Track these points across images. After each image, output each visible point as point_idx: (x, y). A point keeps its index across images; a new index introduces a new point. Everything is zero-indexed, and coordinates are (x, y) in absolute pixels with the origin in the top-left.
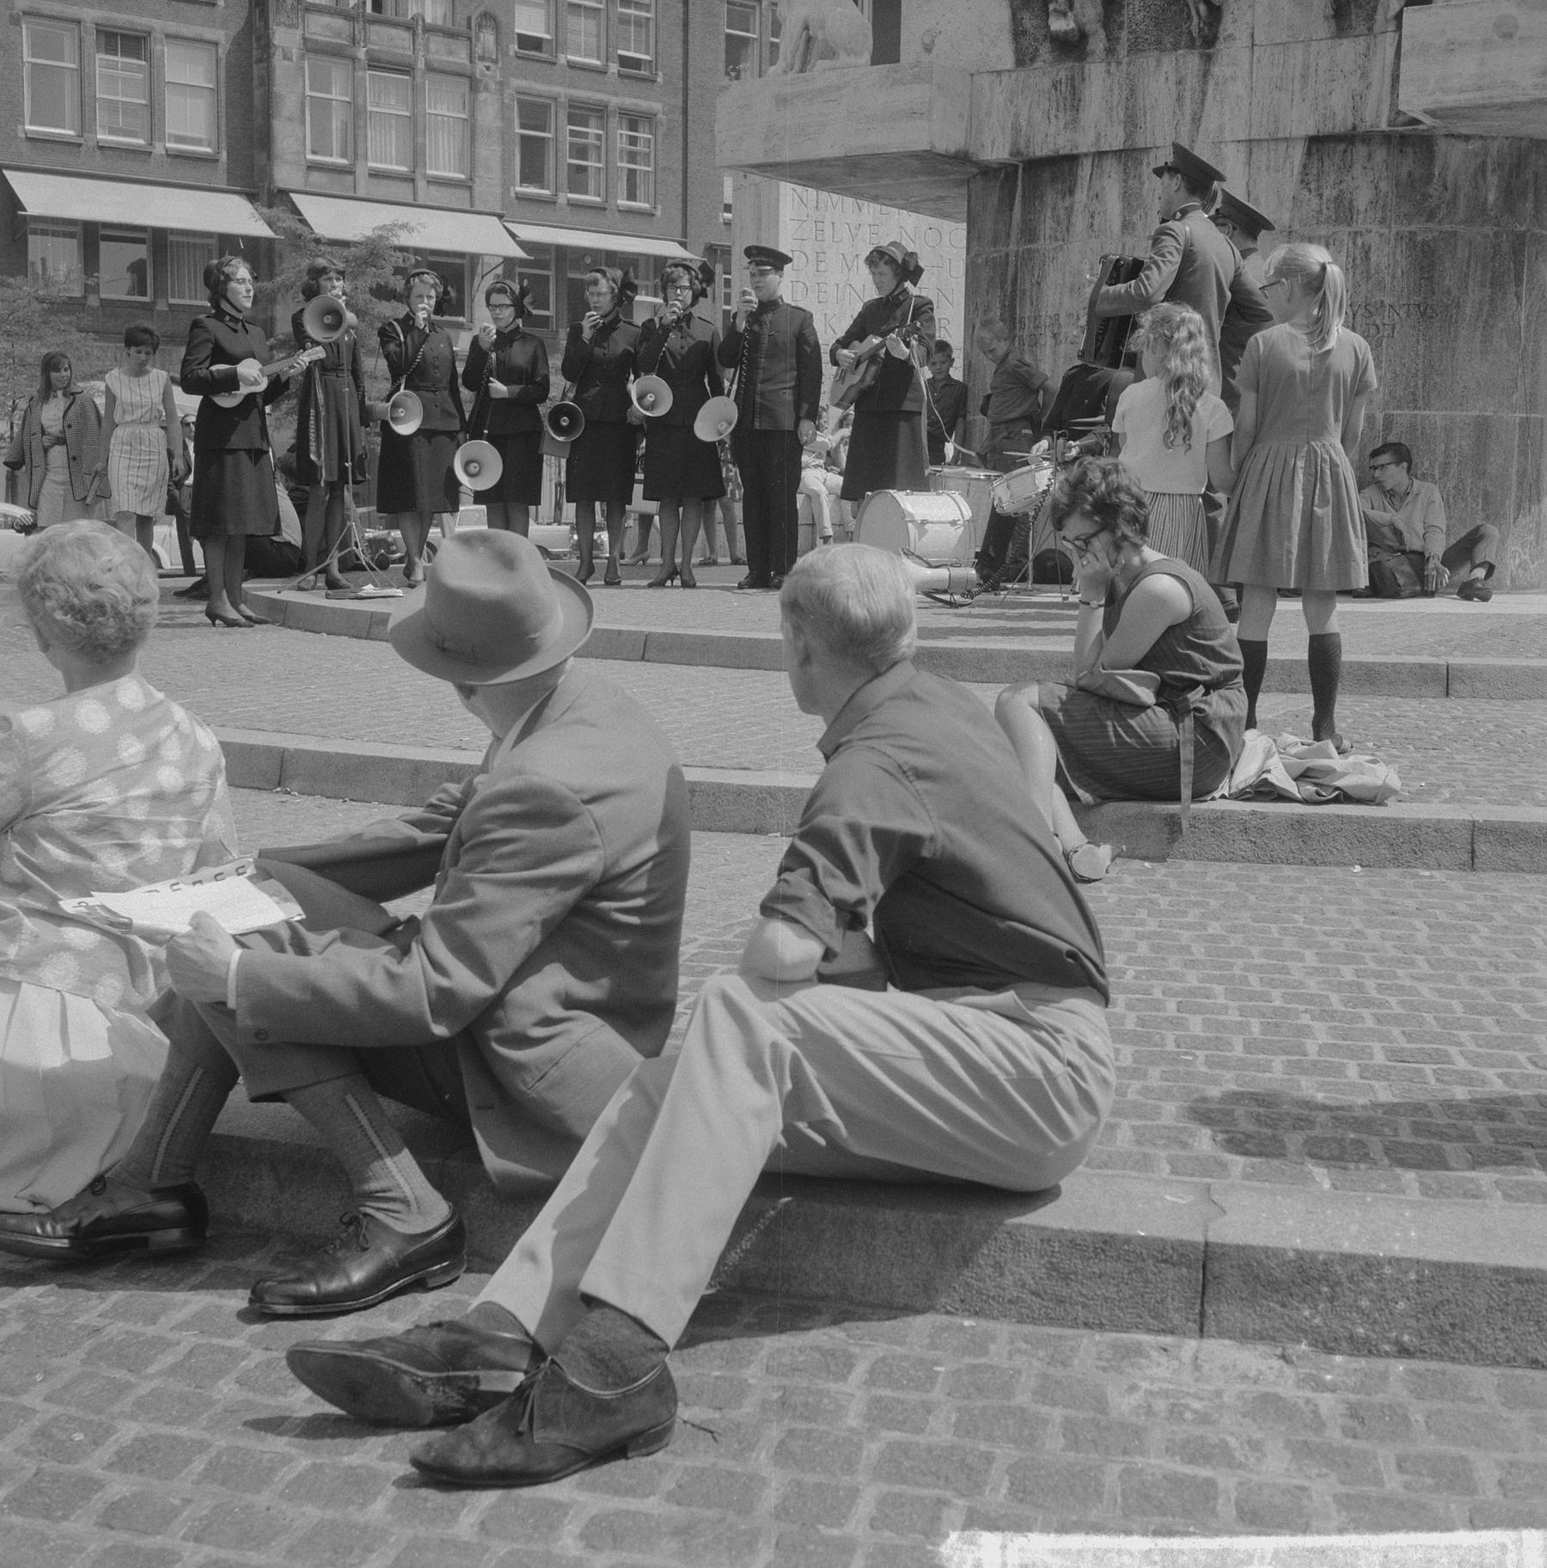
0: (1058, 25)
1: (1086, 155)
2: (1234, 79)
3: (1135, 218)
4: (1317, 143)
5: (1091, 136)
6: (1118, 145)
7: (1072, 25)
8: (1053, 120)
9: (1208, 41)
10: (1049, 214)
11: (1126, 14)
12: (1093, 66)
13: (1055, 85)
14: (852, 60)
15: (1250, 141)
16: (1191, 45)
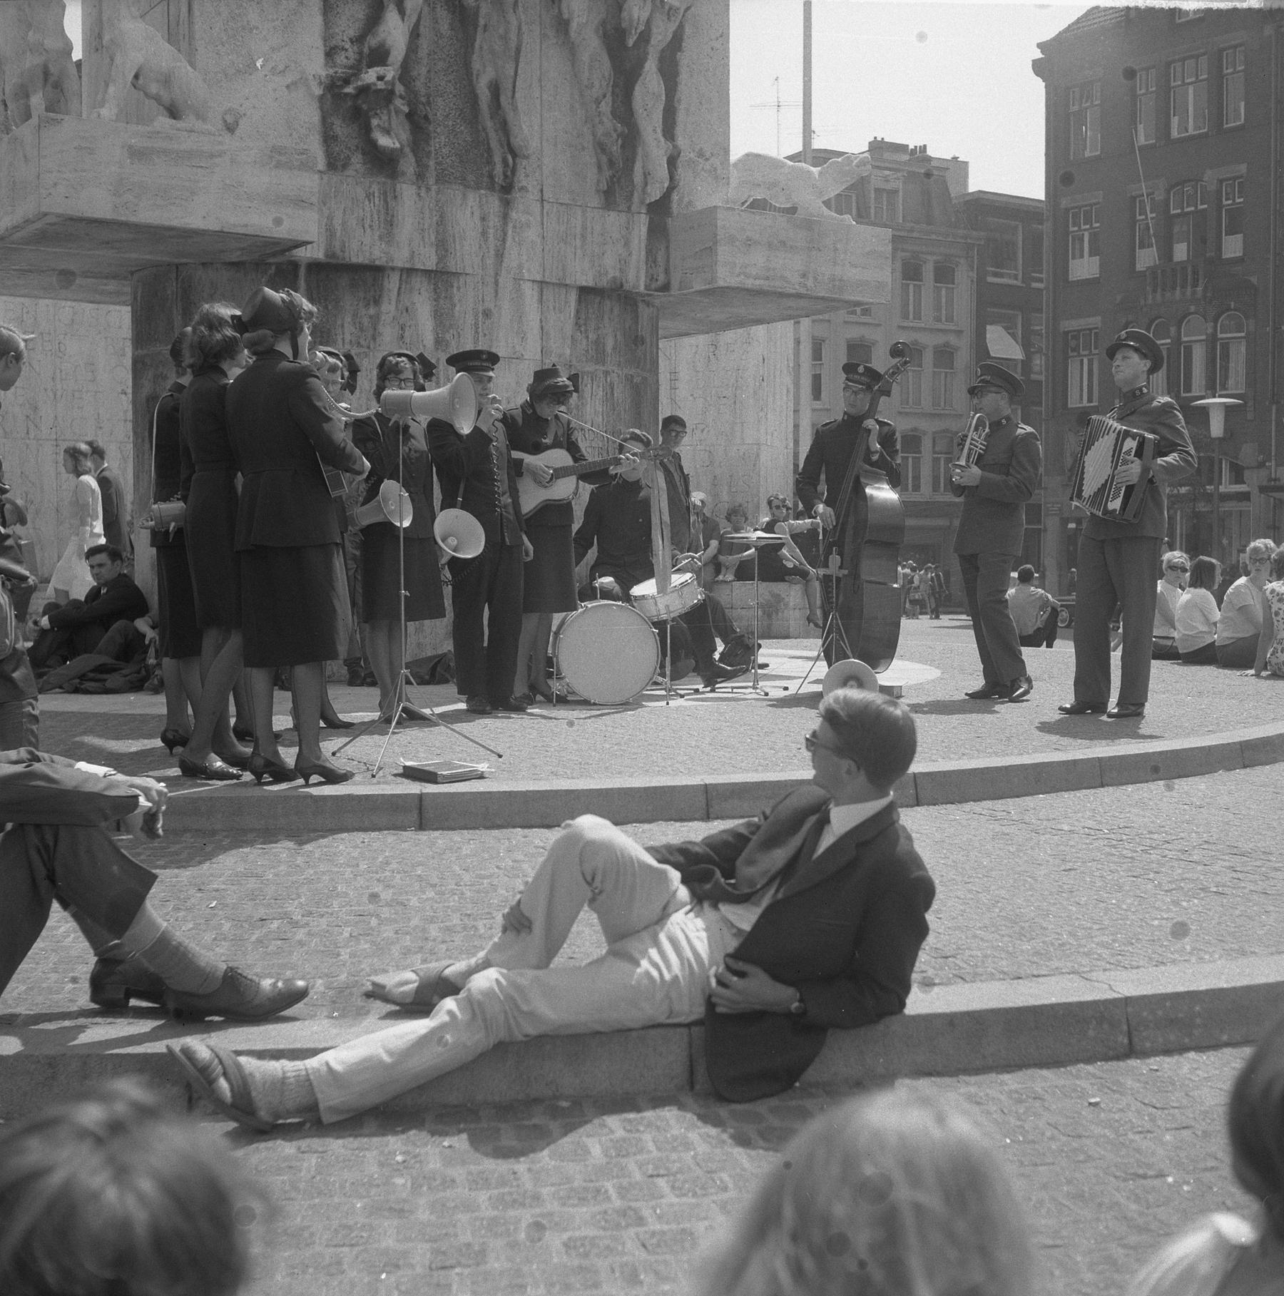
0: (384, 141)
1: (393, 269)
2: (528, 226)
3: (448, 336)
4: (584, 291)
5: (405, 253)
6: (431, 264)
7: (398, 145)
8: (368, 230)
9: (507, 189)
10: (348, 319)
11: (434, 144)
12: (404, 186)
13: (369, 196)
14: (199, 125)
15: (542, 284)
16: (491, 187)
